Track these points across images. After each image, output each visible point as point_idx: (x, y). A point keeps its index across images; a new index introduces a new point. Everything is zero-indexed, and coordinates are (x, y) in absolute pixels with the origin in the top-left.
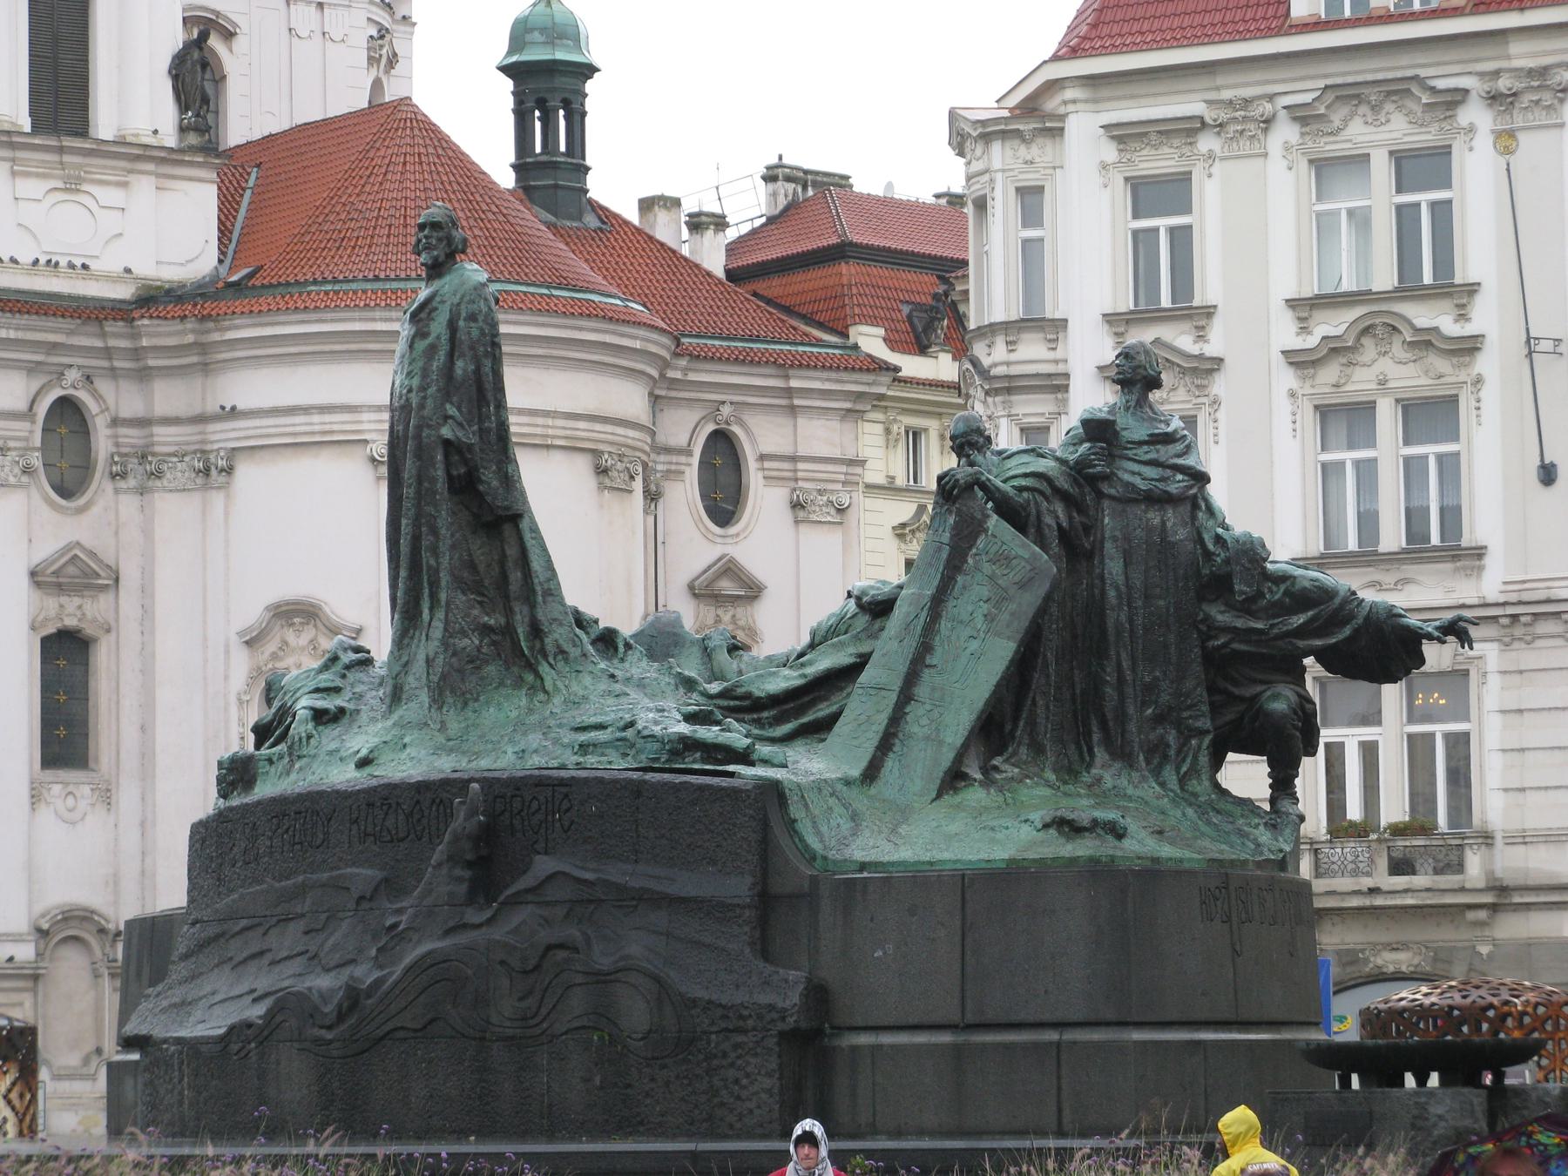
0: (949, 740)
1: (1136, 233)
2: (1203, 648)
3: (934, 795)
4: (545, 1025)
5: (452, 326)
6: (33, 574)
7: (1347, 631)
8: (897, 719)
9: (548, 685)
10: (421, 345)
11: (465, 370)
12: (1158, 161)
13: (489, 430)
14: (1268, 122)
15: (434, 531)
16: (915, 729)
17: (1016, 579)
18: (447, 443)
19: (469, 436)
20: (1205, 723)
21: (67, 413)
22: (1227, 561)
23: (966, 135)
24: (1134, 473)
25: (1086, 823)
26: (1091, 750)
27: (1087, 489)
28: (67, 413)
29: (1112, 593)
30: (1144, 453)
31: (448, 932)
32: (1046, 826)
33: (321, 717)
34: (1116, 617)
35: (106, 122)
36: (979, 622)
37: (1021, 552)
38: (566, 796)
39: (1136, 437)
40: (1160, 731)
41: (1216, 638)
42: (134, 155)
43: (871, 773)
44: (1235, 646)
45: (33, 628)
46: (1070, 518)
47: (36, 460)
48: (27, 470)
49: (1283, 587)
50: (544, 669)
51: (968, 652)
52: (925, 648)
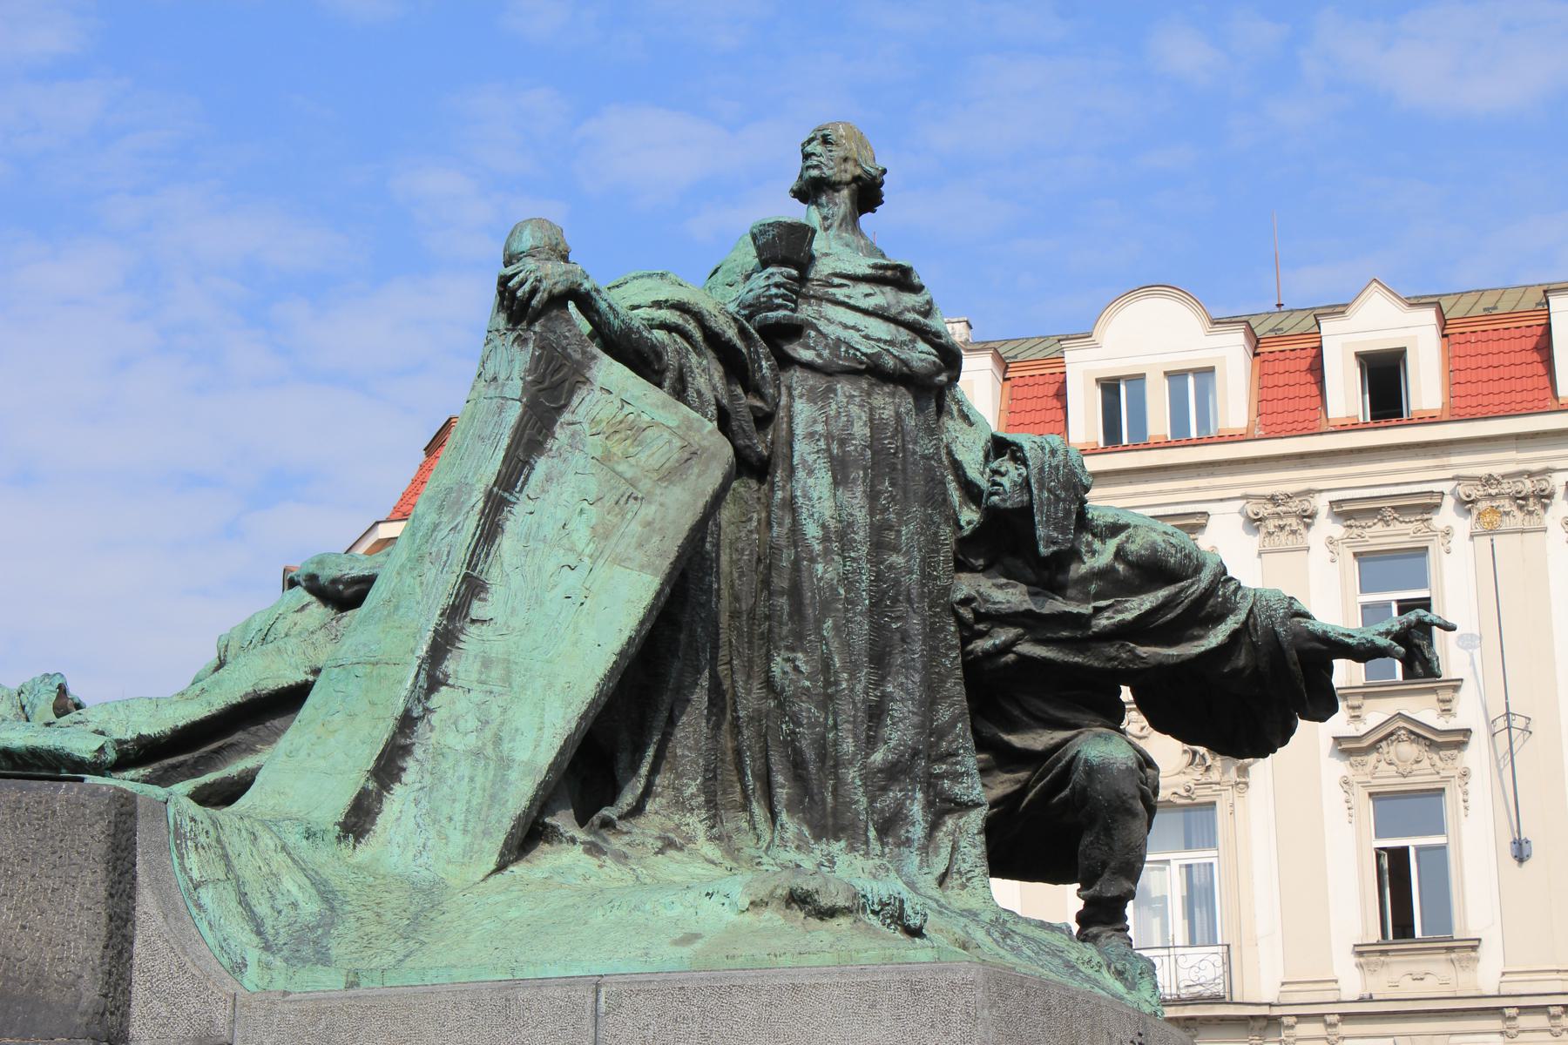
2: (965, 654)
3: (492, 862)
7: (1216, 637)
8: (407, 722)
16: (452, 739)
17: (655, 462)
24: (846, 327)
25: (841, 902)
26: (774, 816)
27: (763, 349)
29: (812, 531)
30: (858, 294)
36: (581, 535)
39: (849, 269)
40: (895, 794)
41: (982, 635)
43: (358, 820)
44: (1026, 648)
46: (733, 397)
49: (1112, 544)
51: (559, 592)
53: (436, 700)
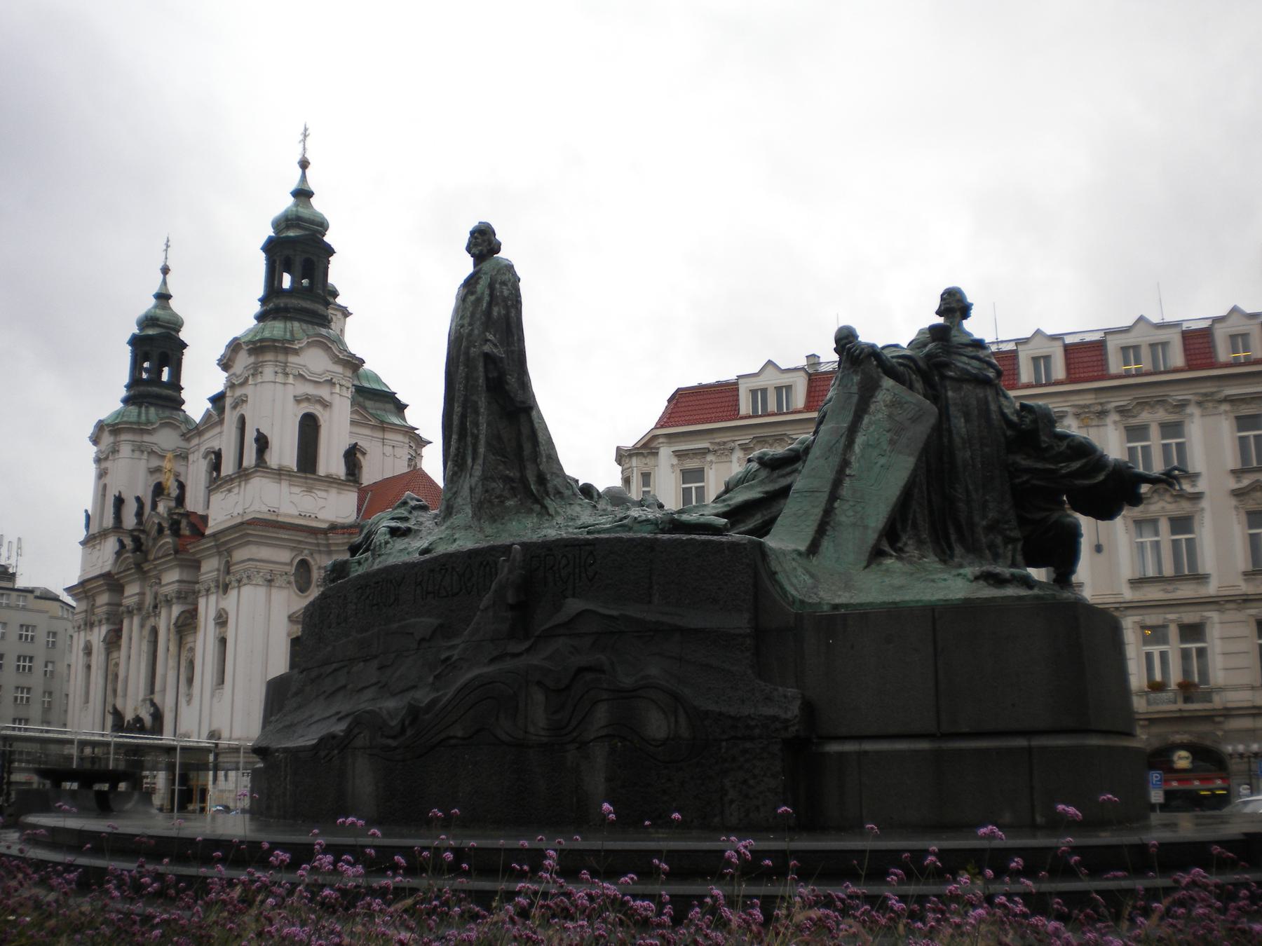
0: (872, 525)
1: (684, 489)
3: (865, 564)
4: (575, 734)
5: (491, 286)
6: (289, 617)
7: (1101, 477)
8: (828, 512)
9: (551, 511)
10: (472, 298)
11: (499, 313)
12: (692, 464)
13: (513, 352)
14: (732, 450)
15: (476, 412)
16: (843, 519)
18: (487, 357)
19: (499, 352)
20: (1016, 534)
21: (304, 565)
22: (1035, 421)
23: (623, 456)
25: (1008, 576)
28: (304, 565)
29: (957, 440)
31: (492, 661)
32: (977, 578)
33: (394, 532)
34: (963, 455)
35: (322, 471)
36: (885, 446)
37: (909, 399)
38: (591, 553)
40: (991, 536)
42: (331, 481)
43: (814, 548)
44: (1035, 482)
45: (289, 635)
47: (292, 579)
48: (289, 583)
49: (1065, 443)
50: (548, 502)
52: (845, 463)
53: (836, 505)
